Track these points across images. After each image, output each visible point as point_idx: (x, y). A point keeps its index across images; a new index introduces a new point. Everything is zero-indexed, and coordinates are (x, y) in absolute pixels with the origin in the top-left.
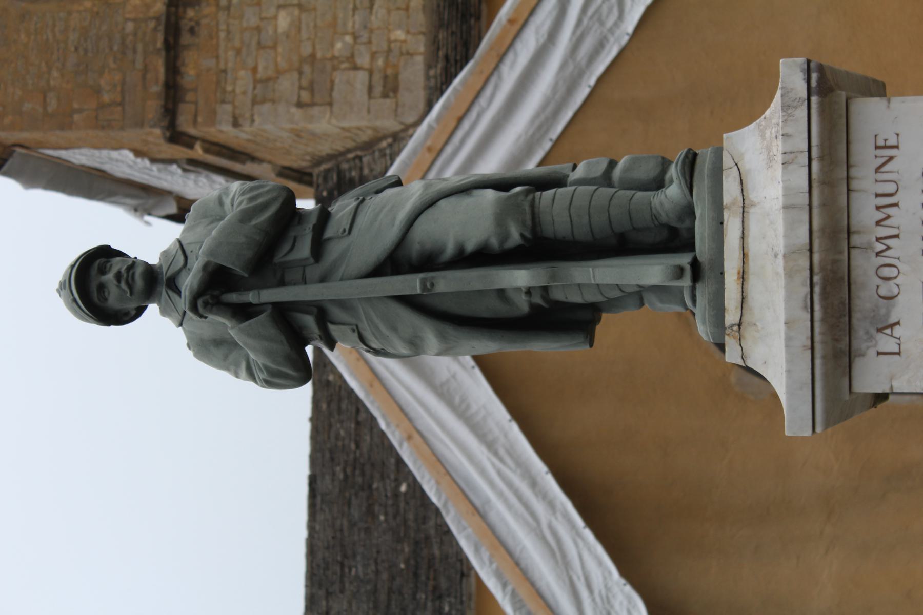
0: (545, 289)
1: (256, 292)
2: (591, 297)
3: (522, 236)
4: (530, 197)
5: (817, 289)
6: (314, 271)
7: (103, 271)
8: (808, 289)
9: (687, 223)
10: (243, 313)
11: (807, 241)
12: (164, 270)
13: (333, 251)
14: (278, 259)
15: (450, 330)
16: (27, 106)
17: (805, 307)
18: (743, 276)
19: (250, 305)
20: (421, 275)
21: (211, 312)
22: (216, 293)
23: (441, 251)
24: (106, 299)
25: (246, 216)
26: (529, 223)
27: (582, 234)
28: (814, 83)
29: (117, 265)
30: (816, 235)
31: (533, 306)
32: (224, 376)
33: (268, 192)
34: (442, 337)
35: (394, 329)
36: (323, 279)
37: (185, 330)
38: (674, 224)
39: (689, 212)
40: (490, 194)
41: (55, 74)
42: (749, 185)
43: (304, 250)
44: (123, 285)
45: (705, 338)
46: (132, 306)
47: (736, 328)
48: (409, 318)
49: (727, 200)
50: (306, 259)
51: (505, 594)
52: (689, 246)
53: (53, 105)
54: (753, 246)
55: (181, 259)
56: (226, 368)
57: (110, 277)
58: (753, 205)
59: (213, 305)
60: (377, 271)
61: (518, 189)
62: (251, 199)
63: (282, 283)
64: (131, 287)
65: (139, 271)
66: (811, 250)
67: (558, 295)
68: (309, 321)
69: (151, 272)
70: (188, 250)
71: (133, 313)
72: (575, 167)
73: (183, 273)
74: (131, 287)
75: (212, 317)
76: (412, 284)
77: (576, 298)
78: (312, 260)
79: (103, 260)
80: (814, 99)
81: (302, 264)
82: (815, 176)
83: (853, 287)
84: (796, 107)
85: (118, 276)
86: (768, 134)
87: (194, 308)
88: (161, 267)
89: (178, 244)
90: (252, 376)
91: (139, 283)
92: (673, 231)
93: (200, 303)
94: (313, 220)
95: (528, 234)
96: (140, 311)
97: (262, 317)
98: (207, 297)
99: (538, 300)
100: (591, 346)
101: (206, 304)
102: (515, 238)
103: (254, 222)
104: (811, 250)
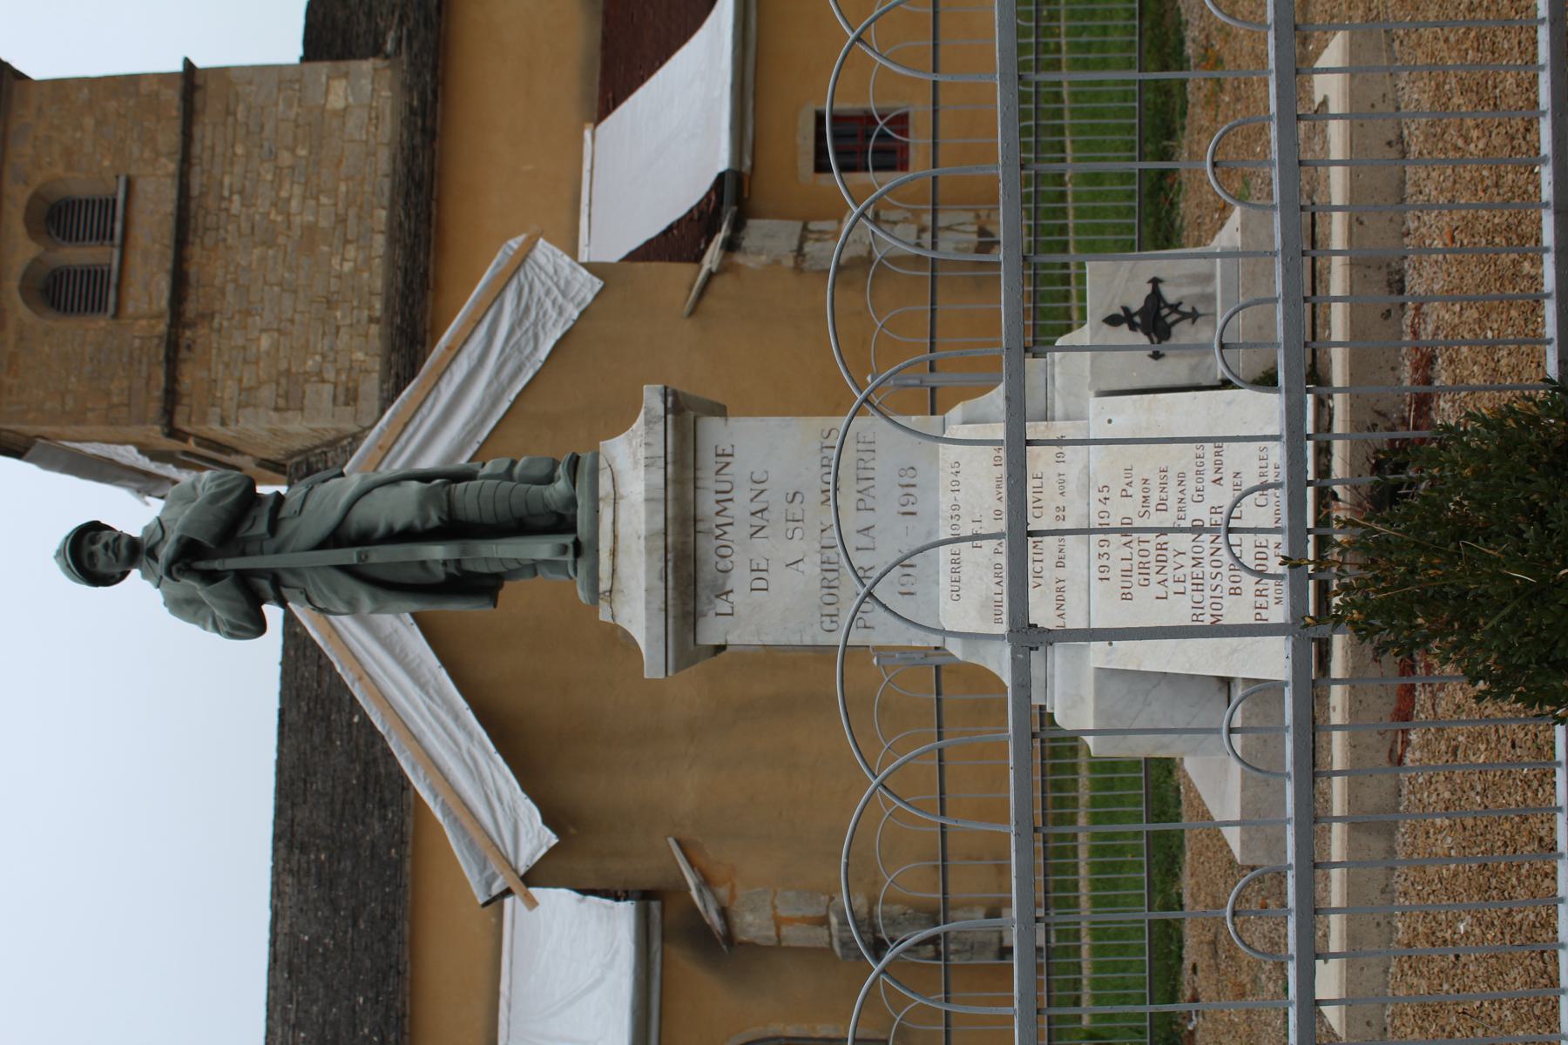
0: (458, 562)
1: (221, 561)
2: (496, 568)
3: (440, 518)
4: (447, 488)
5: (670, 564)
6: (271, 544)
7: (93, 542)
8: (663, 564)
9: (571, 511)
10: (210, 577)
11: (663, 526)
12: (145, 542)
13: (286, 529)
14: (241, 533)
15: (381, 594)
16: (48, 405)
17: (661, 578)
18: (614, 553)
19: (216, 571)
20: (358, 549)
21: (183, 576)
22: (188, 561)
23: (375, 530)
24: (95, 565)
25: (214, 499)
26: (446, 509)
27: (488, 518)
28: (669, 404)
29: (105, 537)
30: (669, 522)
31: (449, 575)
32: (193, 630)
33: (234, 479)
34: (374, 599)
35: (335, 592)
36: (278, 551)
37: (163, 593)
38: (561, 511)
39: (572, 502)
40: (415, 485)
41: (73, 379)
42: (619, 481)
43: (262, 527)
44: (110, 554)
45: (584, 602)
46: (117, 570)
47: (608, 594)
48: (346, 582)
49: (602, 493)
50: (263, 535)
51: (436, 804)
52: (571, 528)
53: (70, 404)
54: (623, 530)
55: (159, 533)
56: (196, 622)
57: (99, 547)
58: (622, 497)
59: (184, 571)
60: (322, 545)
61: (438, 481)
62: (219, 485)
63: (243, 554)
64: (116, 555)
65: (123, 542)
66: (666, 534)
67: (469, 566)
68: (265, 585)
69: (134, 544)
70: (165, 525)
71: (118, 576)
72: (484, 465)
73: (161, 545)
74: (116, 555)
75: (184, 581)
76: (350, 556)
77: (483, 569)
78: (268, 536)
79: (93, 533)
80: (670, 417)
81: (260, 539)
82: (669, 476)
83: (698, 563)
84: (655, 423)
85: (106, 546)
86: (634, 443)
87: (169, 573)
88: (142, 539)
89: (157, 522)
90: (217, 629)
91: (124, 552)
92: (561, 517)
93: (174, 569)
94: (270, 503)
95: (444, 517)
96: (124, 575)
97: (226, 582)
98: (180, 565)
99: (452, 570)
100: (495, 606)
102: (434, 519)
103: (221, 504)
104: (666, 534)
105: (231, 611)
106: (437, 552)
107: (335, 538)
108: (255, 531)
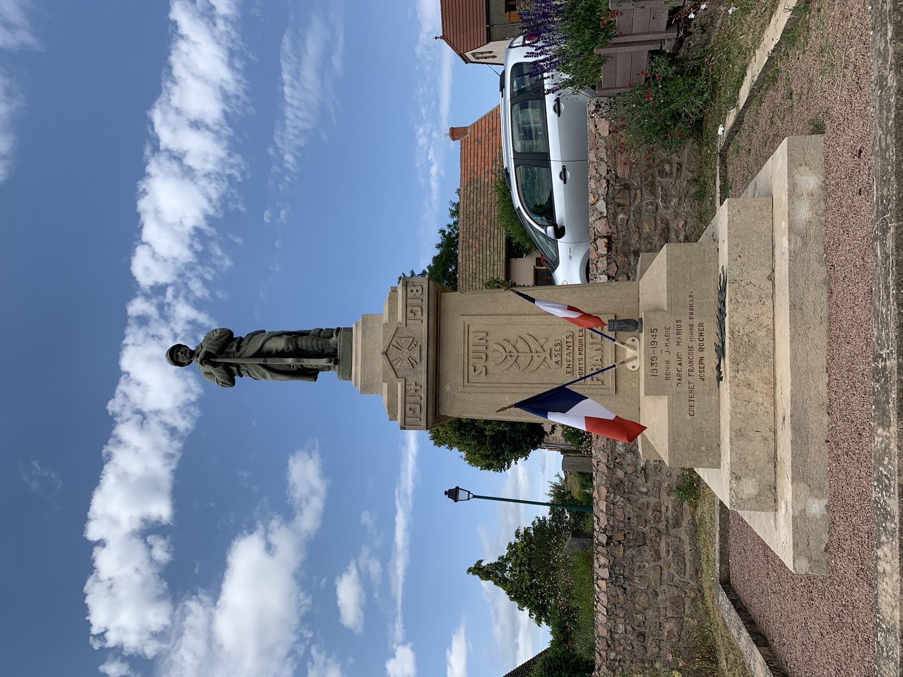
6: (238, 354)
7: (178, 351)
10: (215, 365)
13: (242, 350)
14: (227, 350)
29: (182, 349)
34: (271, 376)
40: (285, 336)
43: (234, 349)
63: (227, 357)
68: (235, 369)
75: (206, 366)
87: (201, 363)
94: (238, 340)
96: (190, 363)
100: (315, 381)
101: (205, 362)
105: (222, 377)
106: (290, 361)
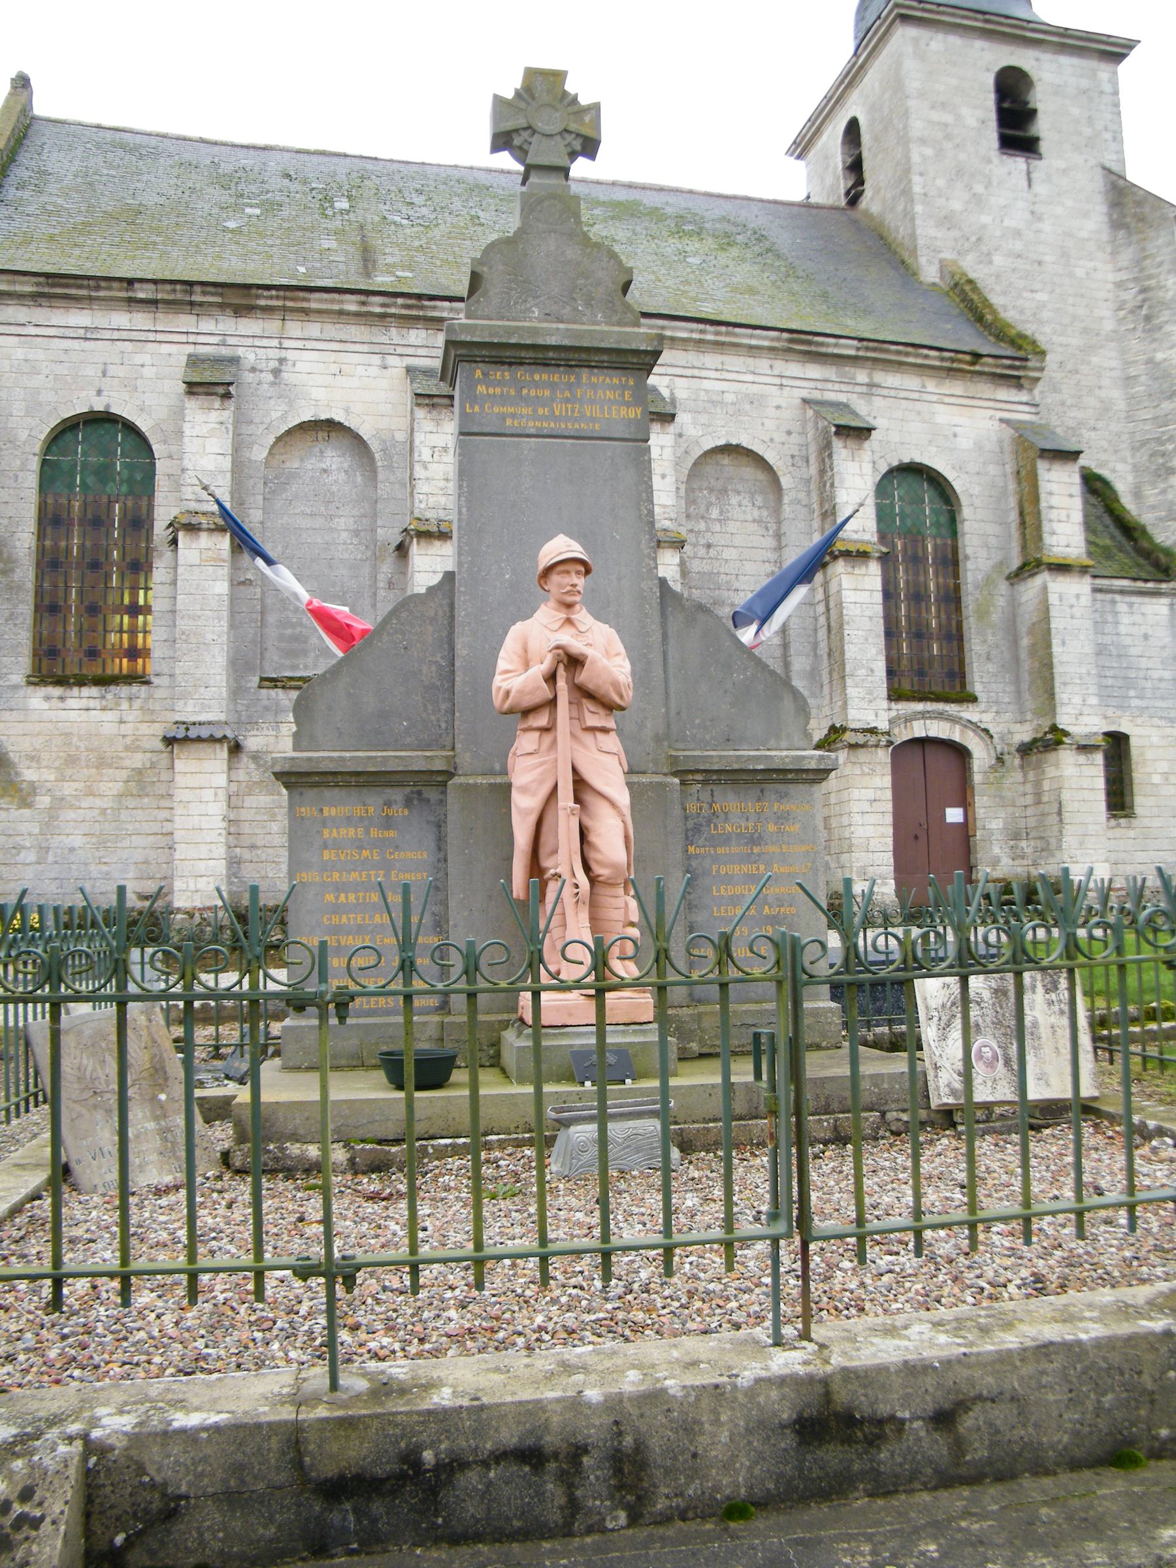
7: (578, 573)
10: (551, 678)
13: (588, 738)
14: (584, 701)
43: (592, 721)
60: (575, 771)
68: (542, 720)
91: (569, 599)
105: (521, 692)
107: (580, 784)
108: (587, 715)
